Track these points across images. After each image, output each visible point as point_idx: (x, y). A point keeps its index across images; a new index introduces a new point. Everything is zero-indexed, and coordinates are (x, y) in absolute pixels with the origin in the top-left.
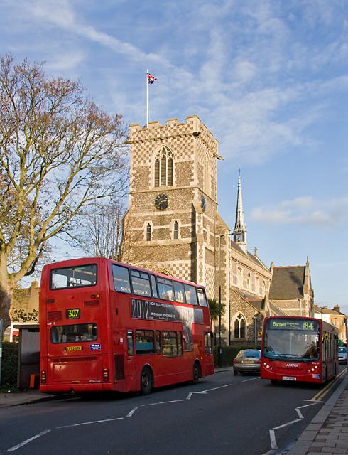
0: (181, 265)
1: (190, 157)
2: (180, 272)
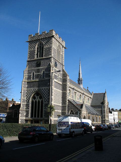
0: (45, 89)
2: (45, 92)
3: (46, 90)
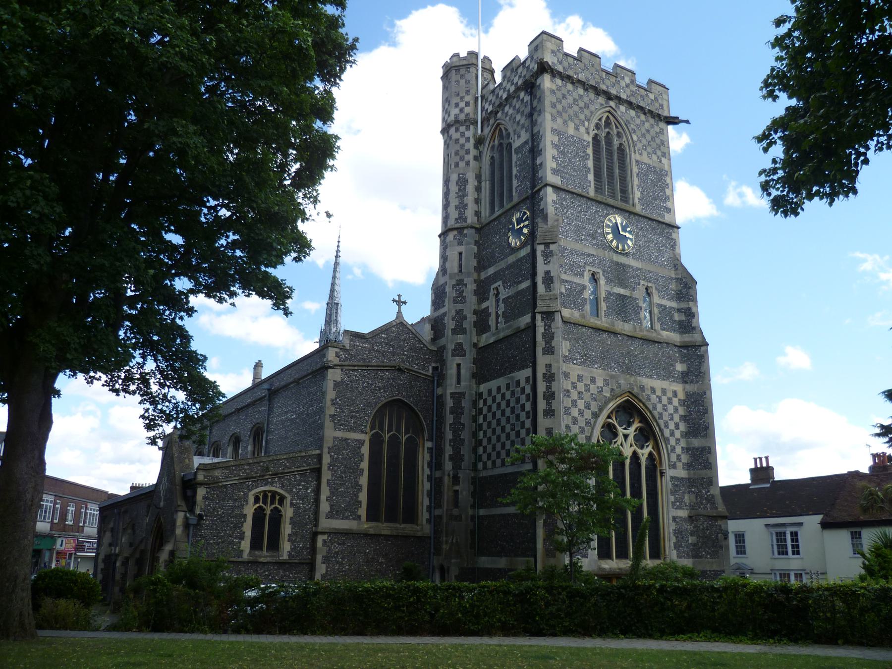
0: (664, 391)
1: (661, 161)
3: (670, 401)
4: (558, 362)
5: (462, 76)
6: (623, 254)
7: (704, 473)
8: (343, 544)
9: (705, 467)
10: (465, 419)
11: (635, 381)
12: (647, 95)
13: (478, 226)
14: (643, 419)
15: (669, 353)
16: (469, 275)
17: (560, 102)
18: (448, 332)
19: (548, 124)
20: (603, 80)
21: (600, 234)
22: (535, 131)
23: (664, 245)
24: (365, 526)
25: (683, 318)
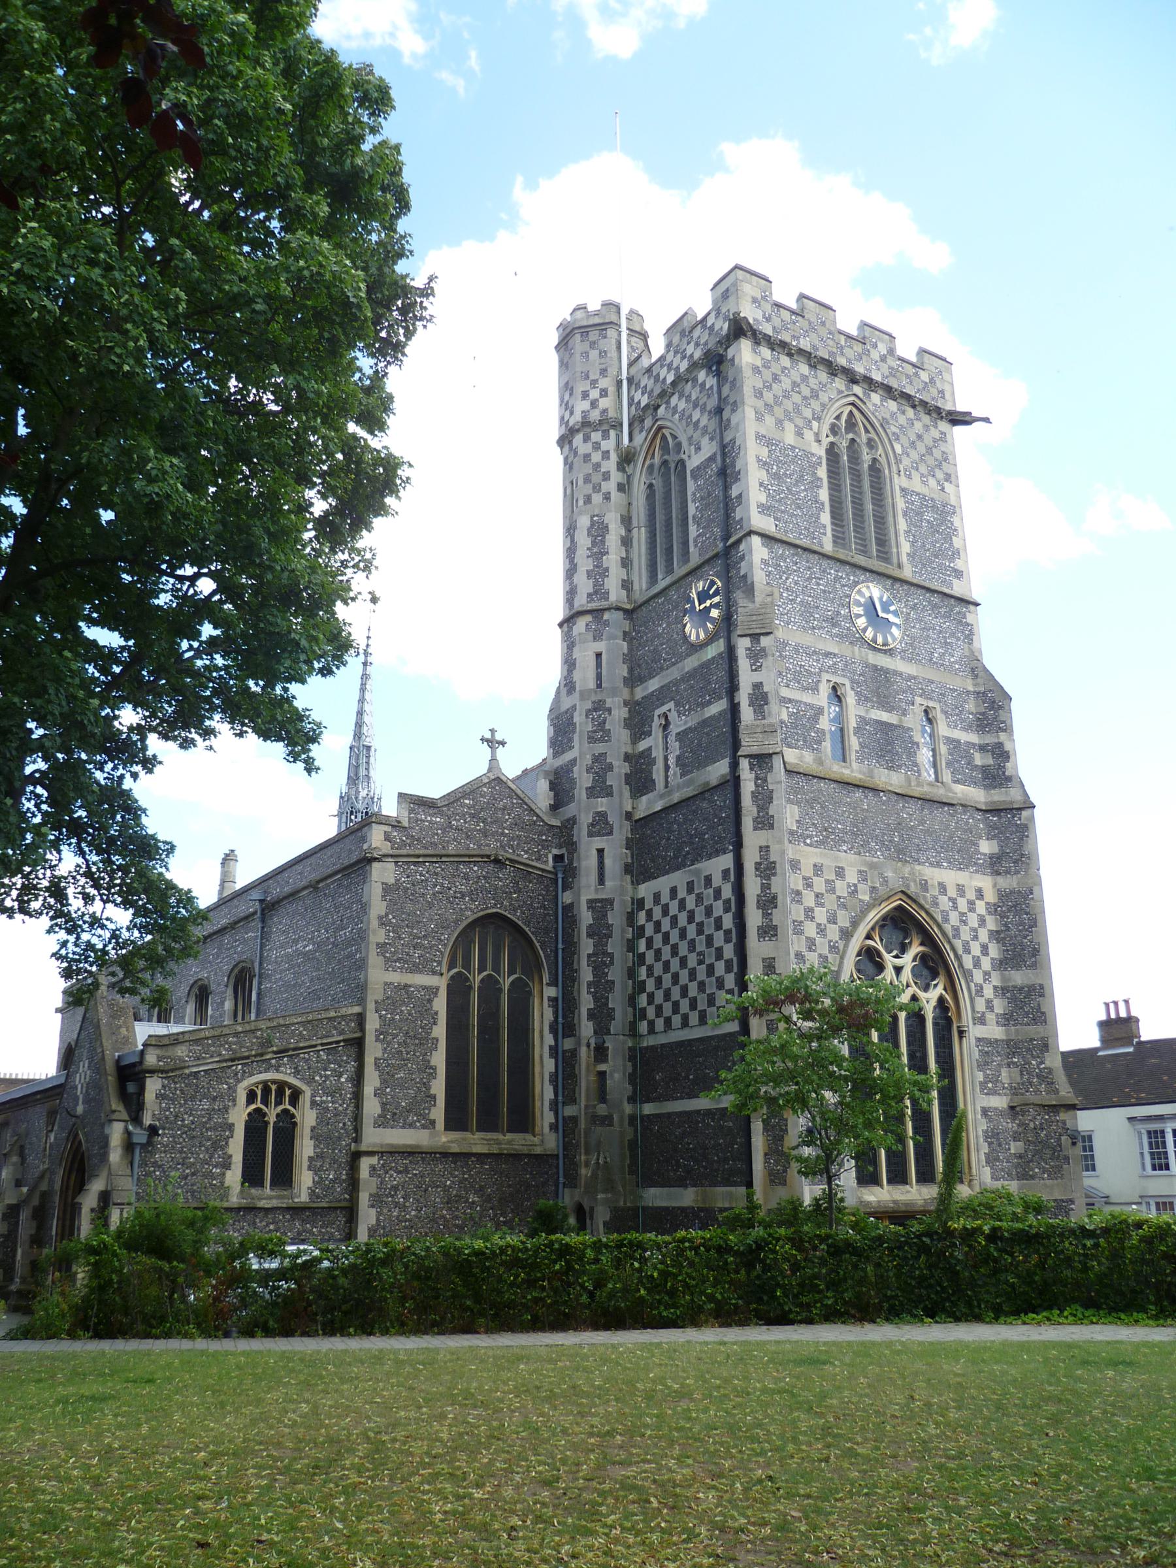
0: (961, 889)
1: (943, 490)
4: (781, 842)
5: (593, 345)
6: (885, 652)
7: (1034, 1030)
8: (406, 1171)
9: (1035, 1021)
10: (615, 946)
11: (912, 873)
12: (916, 375)
13: (628, 607)
14: (928, 939)
15: (967, 823)
16: (614, 692)
17: (770, 388)
18: (581, 794)
19: (751, 427)
20: (842, 348)
21: (845, 617)
22: (727, 440)
23: (953, 635)
24: (444, 1139)
25: (990, 761)
